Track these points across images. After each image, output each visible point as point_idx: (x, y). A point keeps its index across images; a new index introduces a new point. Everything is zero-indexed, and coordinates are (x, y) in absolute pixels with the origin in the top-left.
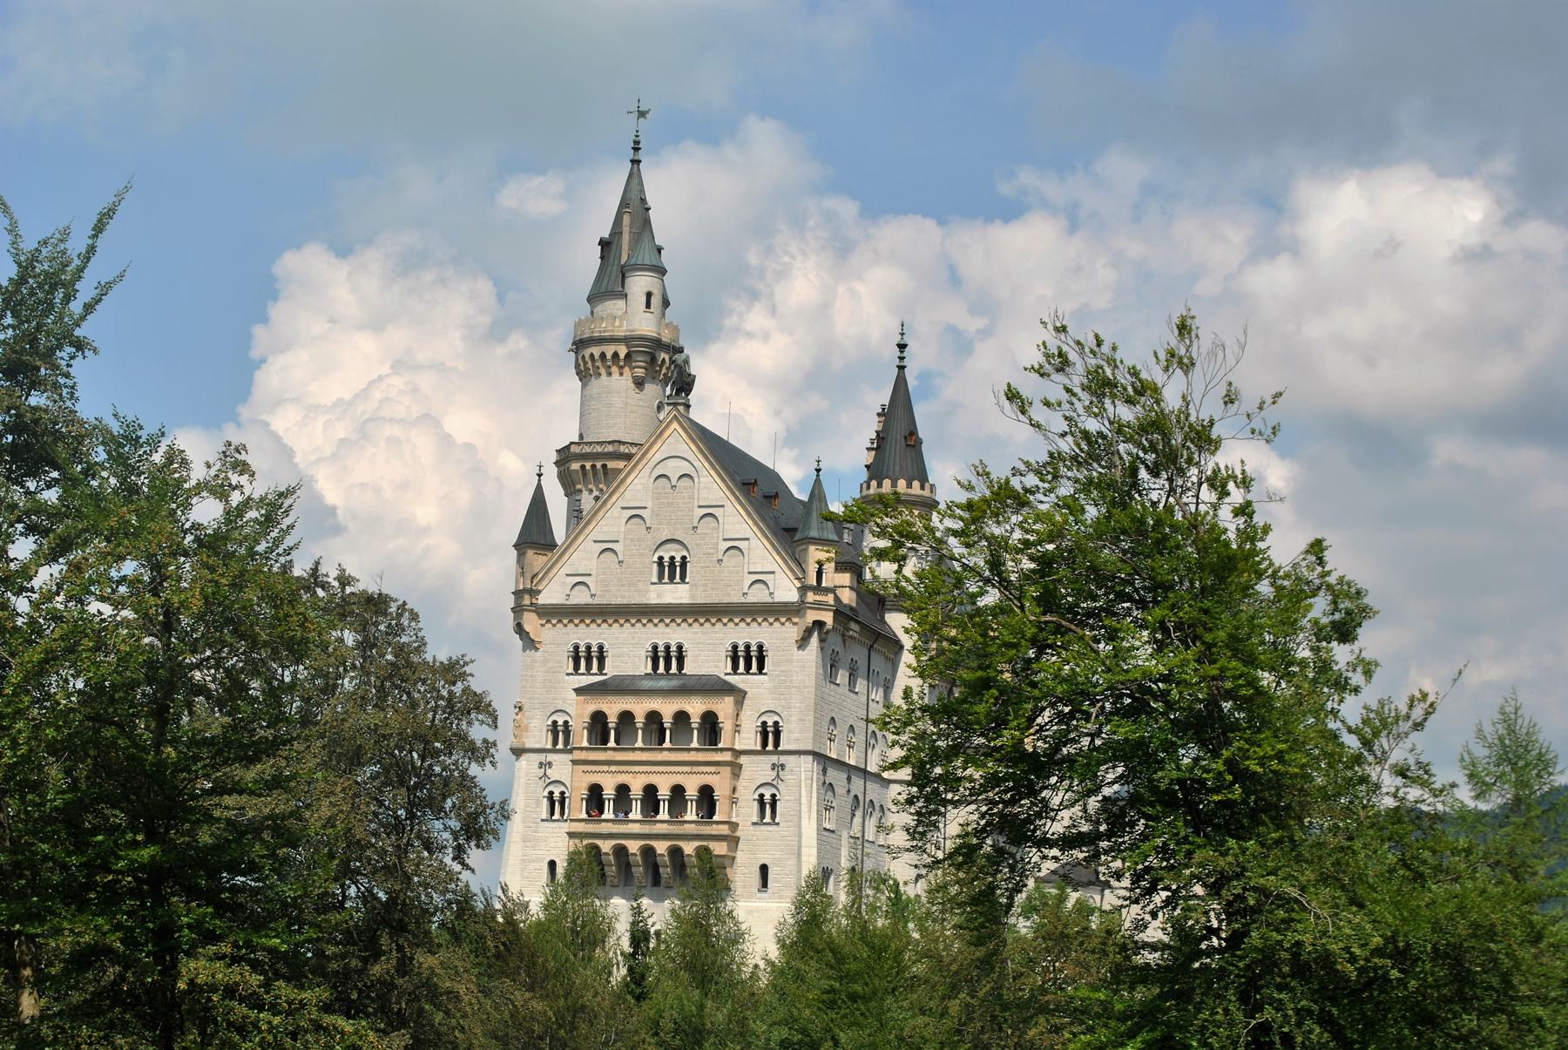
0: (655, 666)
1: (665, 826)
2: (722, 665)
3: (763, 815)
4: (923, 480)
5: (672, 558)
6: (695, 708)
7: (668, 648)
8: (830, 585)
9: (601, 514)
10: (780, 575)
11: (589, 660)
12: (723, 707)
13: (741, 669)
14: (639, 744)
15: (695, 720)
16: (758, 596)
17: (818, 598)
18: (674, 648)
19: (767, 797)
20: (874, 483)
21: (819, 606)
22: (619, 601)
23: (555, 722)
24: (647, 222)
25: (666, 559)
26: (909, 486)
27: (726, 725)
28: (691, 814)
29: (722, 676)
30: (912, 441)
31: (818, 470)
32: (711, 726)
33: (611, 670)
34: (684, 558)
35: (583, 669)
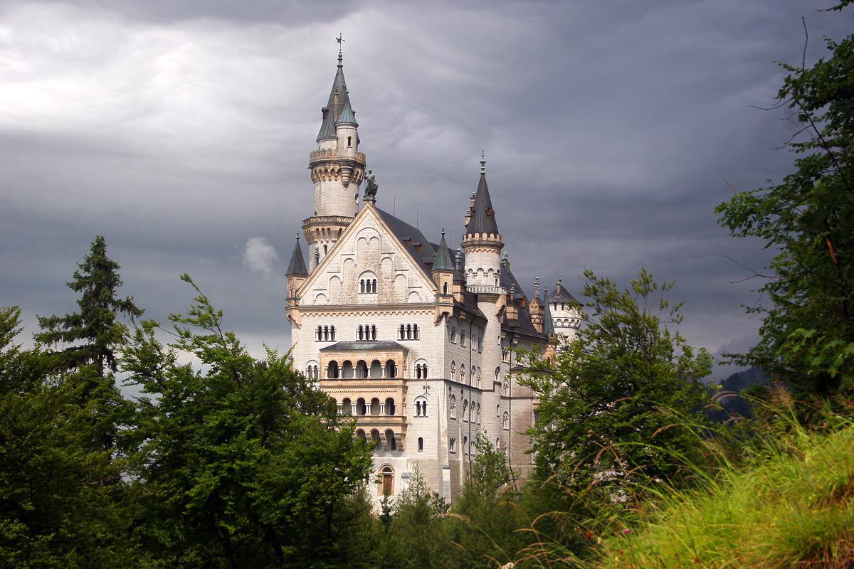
0: (361, 337)
1: (369, 419)
2: (396, 336)
3: (419, 413)
4: (496, 233)
5: (368, 280)
6: (383, 357)
7: (367, 327)
8: (451, 293)
9: (331, 258)
10: (424, 288)
11: (326, 333)
12: (397, 356)
13: (406, 338)
15: (383, 365)
16: (413, 299)
17: (445, 300)
18: (370, 327)
19: (421, 403)
20: (470, 235)
21: (445, 304)
23: (310, 366)
24: (347, 100)
25: (365, 281)
26: (489, 236)
27: (399, 368)
28: (383, 412)
29: (396, 341)
30: (490, 213)
33: (339, 338)
35: (323, 339)
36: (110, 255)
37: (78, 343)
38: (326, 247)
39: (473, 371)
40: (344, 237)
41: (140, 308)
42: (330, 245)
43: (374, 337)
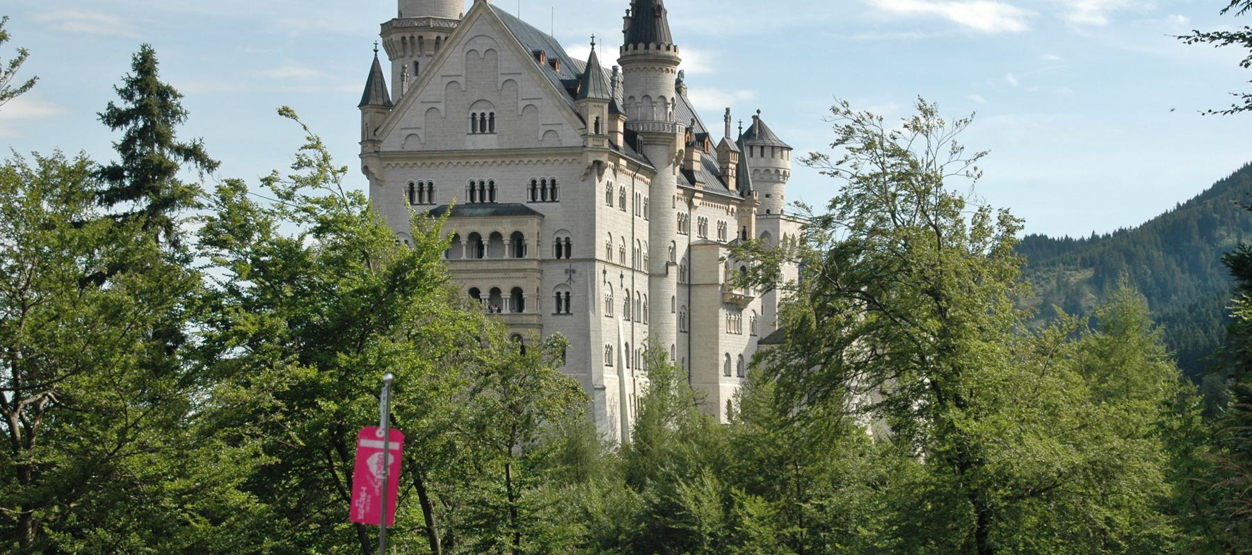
0: (472, 198)
2: (525, 195)
3: (559, 309)
5: (483, 114)
6: (506, 227)
7: (482, 183)
12: (529, 228)
14: (464, 257)
15: (506, 240)
16: (550, 142)
19: (563, 295)
20: (631, 46)
22: (443, 148)
25: (478, 118)
27: (530, 242)
28: (506, 310)
31: (593, 44)
32: (518, 242)
33: (439, 201)
34: (492, 114)
36: (164, 76)
37: (122, 207)
38: (416, 64)
39: (637, 247)
40: (446, 50)
41: (212, 156)
42: (423, 62)
43: (492, 197)
